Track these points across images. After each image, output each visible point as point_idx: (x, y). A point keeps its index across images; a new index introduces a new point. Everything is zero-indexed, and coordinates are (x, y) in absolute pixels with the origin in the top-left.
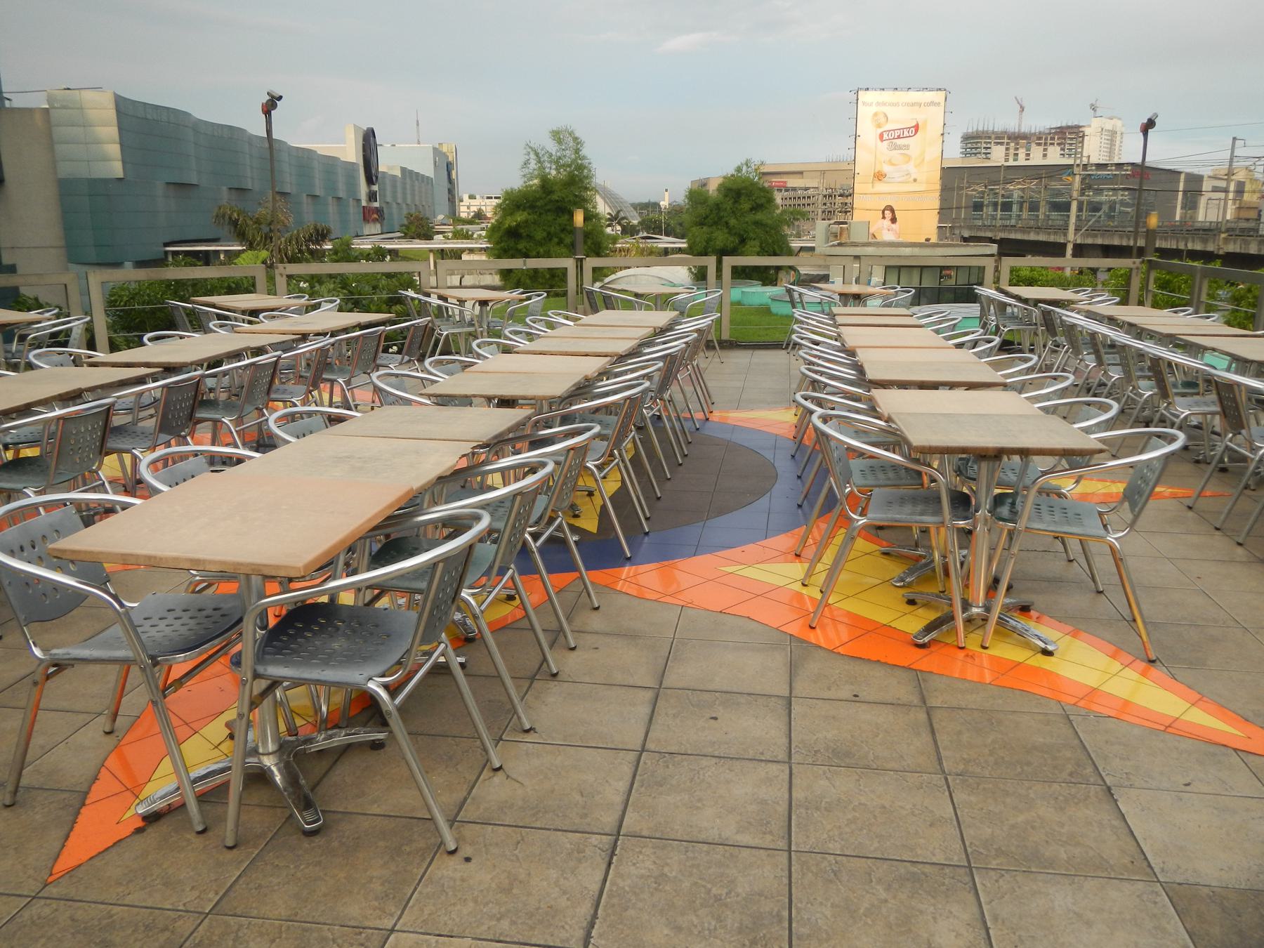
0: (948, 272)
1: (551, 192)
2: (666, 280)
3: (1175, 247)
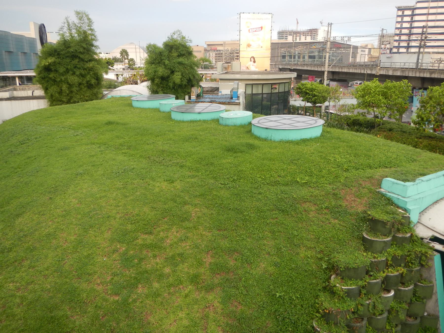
1: (69, 47)
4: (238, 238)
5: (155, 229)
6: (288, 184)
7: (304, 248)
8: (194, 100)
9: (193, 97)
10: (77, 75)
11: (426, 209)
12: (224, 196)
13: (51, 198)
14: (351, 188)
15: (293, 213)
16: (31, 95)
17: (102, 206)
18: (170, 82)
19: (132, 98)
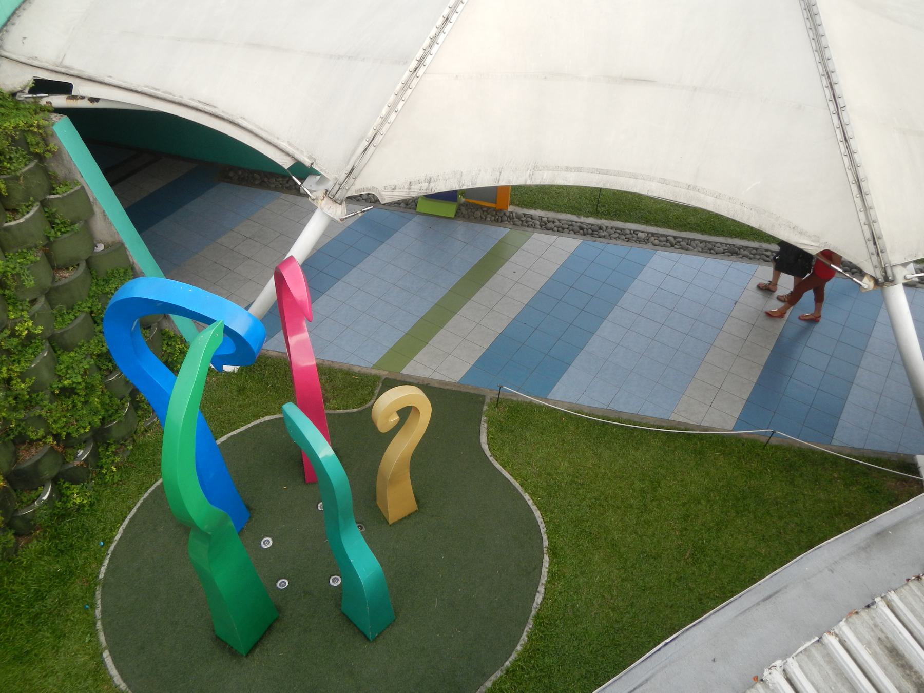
11: (14, 13)
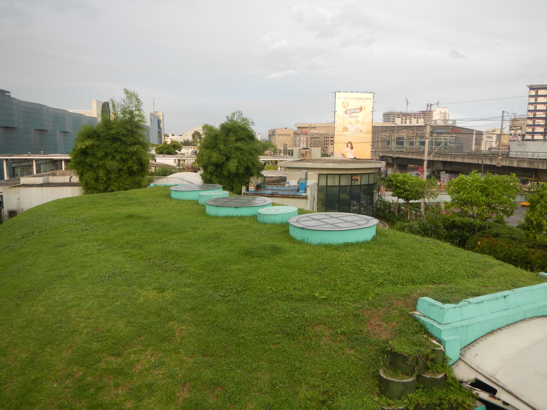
0: (356, 177)
1: (111, 129)
2: (186, 180)
3: (477, 163)
4: (224, 368)
5: (125, 349)
6: (303, 300)
7: (307, 386)
8: (253, 191)
9: (252, 188)
10: (117, 160)
11: (475, 341)
12: (220, 312)
13: (17, 304)
14: (379, 308)
15: (300, 338)
16: (68, 181)
17: (71, 317)
18: (225, 170)
19: (171, 188)
